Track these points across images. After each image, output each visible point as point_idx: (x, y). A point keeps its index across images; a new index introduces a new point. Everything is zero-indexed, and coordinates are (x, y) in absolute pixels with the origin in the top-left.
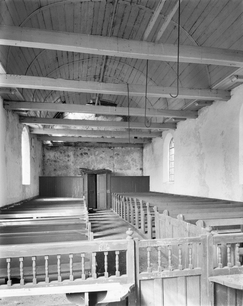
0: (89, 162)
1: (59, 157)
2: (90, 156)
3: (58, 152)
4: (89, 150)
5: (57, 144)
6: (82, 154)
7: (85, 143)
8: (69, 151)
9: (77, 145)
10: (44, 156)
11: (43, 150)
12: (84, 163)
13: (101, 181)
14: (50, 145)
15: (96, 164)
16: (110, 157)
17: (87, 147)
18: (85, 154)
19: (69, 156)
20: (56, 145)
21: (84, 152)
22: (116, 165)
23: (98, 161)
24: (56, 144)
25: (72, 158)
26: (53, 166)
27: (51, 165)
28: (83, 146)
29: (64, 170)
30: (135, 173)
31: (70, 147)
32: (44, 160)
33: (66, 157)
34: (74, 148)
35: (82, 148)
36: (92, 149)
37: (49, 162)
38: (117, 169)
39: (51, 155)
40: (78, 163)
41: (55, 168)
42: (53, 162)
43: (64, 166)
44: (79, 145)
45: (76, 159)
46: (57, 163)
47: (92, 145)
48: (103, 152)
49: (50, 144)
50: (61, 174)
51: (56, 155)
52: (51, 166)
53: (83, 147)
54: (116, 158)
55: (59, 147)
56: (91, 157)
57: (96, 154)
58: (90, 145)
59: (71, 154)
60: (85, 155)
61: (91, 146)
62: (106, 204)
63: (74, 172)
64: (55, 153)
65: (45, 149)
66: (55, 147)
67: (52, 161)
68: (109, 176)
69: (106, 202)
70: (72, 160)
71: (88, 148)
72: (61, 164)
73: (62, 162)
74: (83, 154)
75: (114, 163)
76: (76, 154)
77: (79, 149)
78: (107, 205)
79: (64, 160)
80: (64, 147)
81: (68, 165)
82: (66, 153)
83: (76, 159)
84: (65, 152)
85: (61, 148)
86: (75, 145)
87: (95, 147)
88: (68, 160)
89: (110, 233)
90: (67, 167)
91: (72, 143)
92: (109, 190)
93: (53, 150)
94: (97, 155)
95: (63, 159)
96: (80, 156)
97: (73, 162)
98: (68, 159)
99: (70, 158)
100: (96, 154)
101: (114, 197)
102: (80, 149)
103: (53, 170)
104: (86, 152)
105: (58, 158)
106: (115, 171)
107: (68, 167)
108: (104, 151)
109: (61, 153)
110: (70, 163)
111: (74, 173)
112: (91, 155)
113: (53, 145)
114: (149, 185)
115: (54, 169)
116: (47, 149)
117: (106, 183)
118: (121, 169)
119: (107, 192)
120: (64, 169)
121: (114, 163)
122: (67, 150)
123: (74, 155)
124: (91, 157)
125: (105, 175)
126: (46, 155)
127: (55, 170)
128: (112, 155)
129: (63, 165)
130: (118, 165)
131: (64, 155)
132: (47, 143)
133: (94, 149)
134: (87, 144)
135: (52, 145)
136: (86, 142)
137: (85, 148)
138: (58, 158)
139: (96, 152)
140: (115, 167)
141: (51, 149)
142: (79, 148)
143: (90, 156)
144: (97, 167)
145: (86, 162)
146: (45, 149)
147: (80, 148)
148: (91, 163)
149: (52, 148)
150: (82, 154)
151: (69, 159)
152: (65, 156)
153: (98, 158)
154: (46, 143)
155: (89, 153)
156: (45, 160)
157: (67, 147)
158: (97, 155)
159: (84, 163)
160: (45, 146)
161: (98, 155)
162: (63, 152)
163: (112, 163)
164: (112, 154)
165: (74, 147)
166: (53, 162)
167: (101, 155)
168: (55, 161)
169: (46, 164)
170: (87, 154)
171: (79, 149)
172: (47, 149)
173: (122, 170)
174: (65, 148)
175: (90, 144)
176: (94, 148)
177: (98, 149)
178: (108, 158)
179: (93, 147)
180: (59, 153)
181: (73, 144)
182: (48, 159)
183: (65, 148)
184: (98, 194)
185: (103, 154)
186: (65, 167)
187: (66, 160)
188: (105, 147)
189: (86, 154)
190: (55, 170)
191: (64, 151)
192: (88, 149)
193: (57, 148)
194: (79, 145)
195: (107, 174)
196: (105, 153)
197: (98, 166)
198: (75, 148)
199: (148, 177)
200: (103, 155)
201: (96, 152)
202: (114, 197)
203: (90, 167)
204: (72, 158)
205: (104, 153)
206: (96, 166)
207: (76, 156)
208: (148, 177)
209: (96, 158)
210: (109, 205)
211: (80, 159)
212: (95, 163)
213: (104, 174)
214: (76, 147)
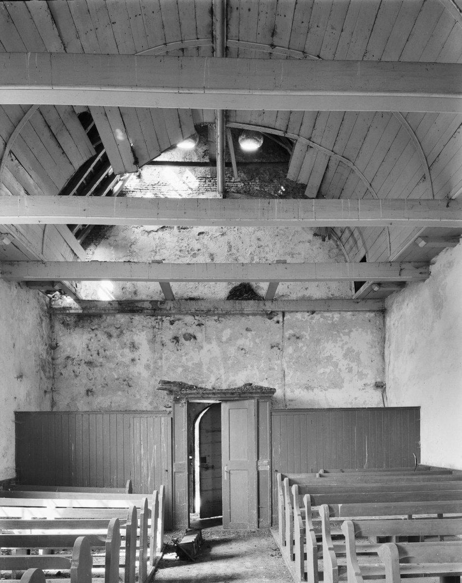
0: (199, 365)
1: (101, 351)
2: (204, 344)
3: (98, 332)
4: (199, 325)
5: (96, 307)
6: (176, 339)
7: (186, 300)
8: (134, 330)
9: (161, 309)
10: (53, 347)
11: (52, 327)
12: (186, 369)
13: (236, 429)
14: (72, 311)
15: (222, 371)
16: (272, 347)
17: (193, 315)
18: (186, 339)
19: (133, 346)
20: (93, 311)
21: (183, 331)
22: (290, 374)
23: (230, 362)
24: (91, 308)
25: (145, 353)
26: (84, 381)
27: (76, 376)
28: (180, 312)
29: (120, 393)
30: (356, 398)
31: (137, 318)
32: (53, 359)
33: (127, 351)
34: (151, 321)
35: (179, 320)
36: (210, 323)
37: (70, 368)
38: (294, 389)
39: (75, 342)
40: (165, 369)
41: (90, 386)
42: (84, 366)
43: (118, 379)
44: (168, 308)
45: (157, 355)
46: (96, 369)
47: (210, 306)
48: (247, 330)
49: (73, 306)
50: (111, 406)
51: (94, 346)
52: (76, 381)
53: (177, 317)
54: (290, 350)
55: (104, 317)
56: (207, 347)
57: (224, 339)
58: (202, 308)
59: (142, 338)
60: (187, 343)
61: (208, 313)
62: (255, 512)
63: (150, 400)
64: (89, 336)
65: (58, 326)
66: (89, 314)
67: (79, 364)
68: (266, 407)
69: (256, 504)
70: (144, 361)
71: (196, 318)
72: (109, 372)
73: (112, 365)
74: (182, 340)
75: (285, 365)
76: (158, 339)
77: (166, 323)
78: (259, 517)
79: (120, 359)
80: (118, 316)
81: (130, 376)
82: (127, 338)
83: (157, 355)
84: (122, 332)
85: (109, 319)
86: (155, 310)
87: (219, 315)
88: (133, 360)
89: (257, 483)
90: (128, 383)
91: (144, 301)
92: (266, 462)
93: (83, 327)
94: (227, 342)
95: (114, 357)
96: (171, 345)
97: (147, 367)
98: (131, 356)
99: (138, 353)
100: (224, 339)
101: (284, 495)
102: (172, 323)
103: (83, 391)
104: (191, 331)
105: (98, 354)
106: (289, 395)
107: (131, 383)
108: (249, 327)
109: (110, 336)
110: (140, 370)
111: (151, 403)
112: (208, 340)
113: (83, 309)
114: (419, 439)
115: (88, 391)
116: (65, 324)
117: (254, 433)
118: (308, 388)
119: (260, 469)
120: (119, 389)
121: (285, 365)
122: (130, 326)
123: (152, 341)
124: (207, 347)
125: (251, 404)
126: (60, 344)
127: (89, 393)
128: (277, 338)
129: (116, 377)
130: (298, 373)
131: (118, 345)
132: (63, 305)
133: (215, 320)
134: (193, 306)
135: (81, 311)
136: (191, 299)
137: (189, 319)
138: (98, 354)
139: (222, 331)
140: (288, 379)
141: (76, 325)
142: (167, 320)
143: (204, 344)
144: (226, 381)
145: (190, 364)
146: (58, 326)
147: (172, 319)
148: (209, 368)
149: (79, 321)
150: (176, 339)
151: (136, 355)
152: (124, 345)
153: (232, 351)
154: (60, 303)
155: (199, 336)
156: (58, 361)
157: (130, 315)
158: (227, 342)
159: (186, 369)
160: (52, 313)
161: (230, 339)
162: (114, 332)
163: (276, 368)
164: (278, 336)
165: (153, 316)
166: (84, 368)
167: (241, 342)
168: (90, 363)
169: (61, 374)
170: (195, 338)
171: (166, 323)
172: (63, 323)
173: (313, 390)
174: (122, 319)
175: (203, 306)
176: (216, 318)
177: (230, 321)
178: (264, 351)
179: (214, 315)
180: (103, 338)
181: (147, 305)
182: (68, 357)
183: (122, 320)
184: (225, 473)
185: (246, 338)
186: (122, 382)
187: (127, 360)
188: (254, 314)
189: (191, 337)
190: (89, 392)
191: (118, 332)
192: (197, 323)
193: (96, 321)
194: (168, 308)
195: (258, 402)
196: (253, 333)
197: (232, 378)
198: (153, 318)
199: (413, 413)
200: (246, 341)
201: (225, 332)
202: (284, 495)
203: (203, 382)
204: (145, 353)
205: (249, 334)
206: (223, 377)
207: (158, 346)
208: (413, 413)
209: (224, 353)
210: (266, 519)
211: (169, 353)
212: (219, 369)
213: (247, 402)
214: (159, 317)
